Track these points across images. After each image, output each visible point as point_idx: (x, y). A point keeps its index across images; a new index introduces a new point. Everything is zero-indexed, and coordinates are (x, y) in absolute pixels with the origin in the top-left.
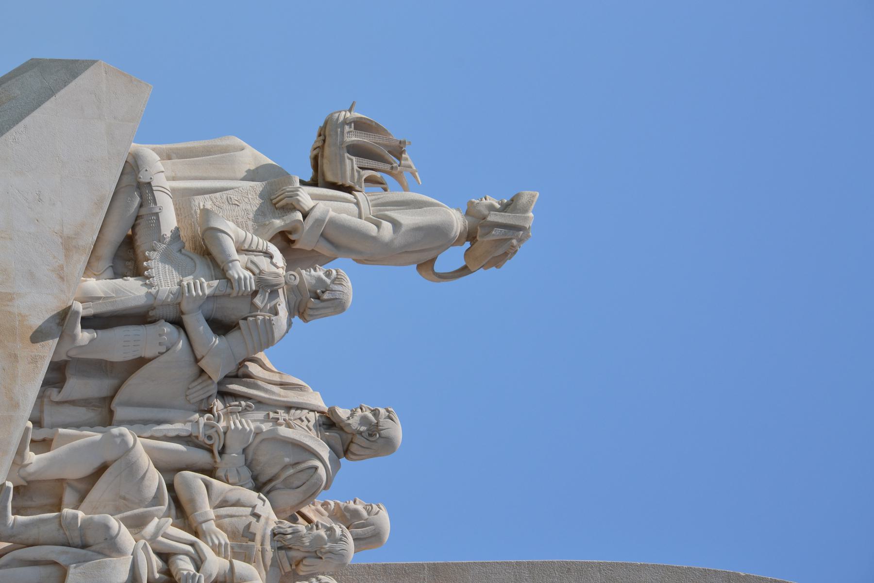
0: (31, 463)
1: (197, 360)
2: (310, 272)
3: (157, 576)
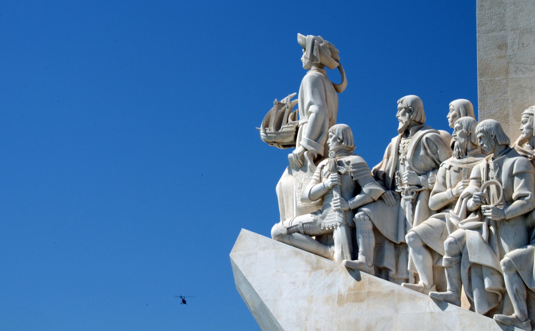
0: (423, 283)
1: (374, 201)
2: (330, 146)
3: (477, 216)
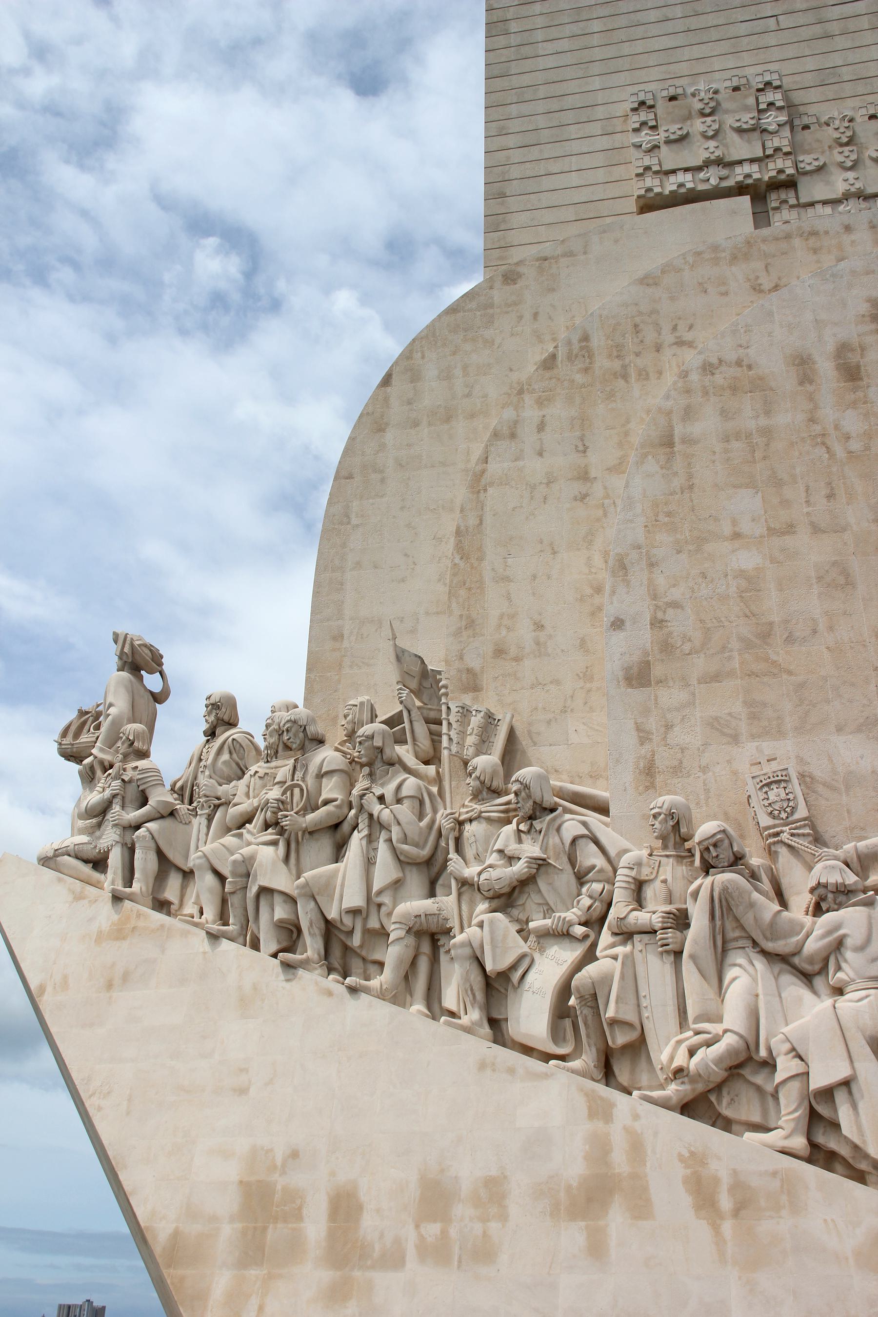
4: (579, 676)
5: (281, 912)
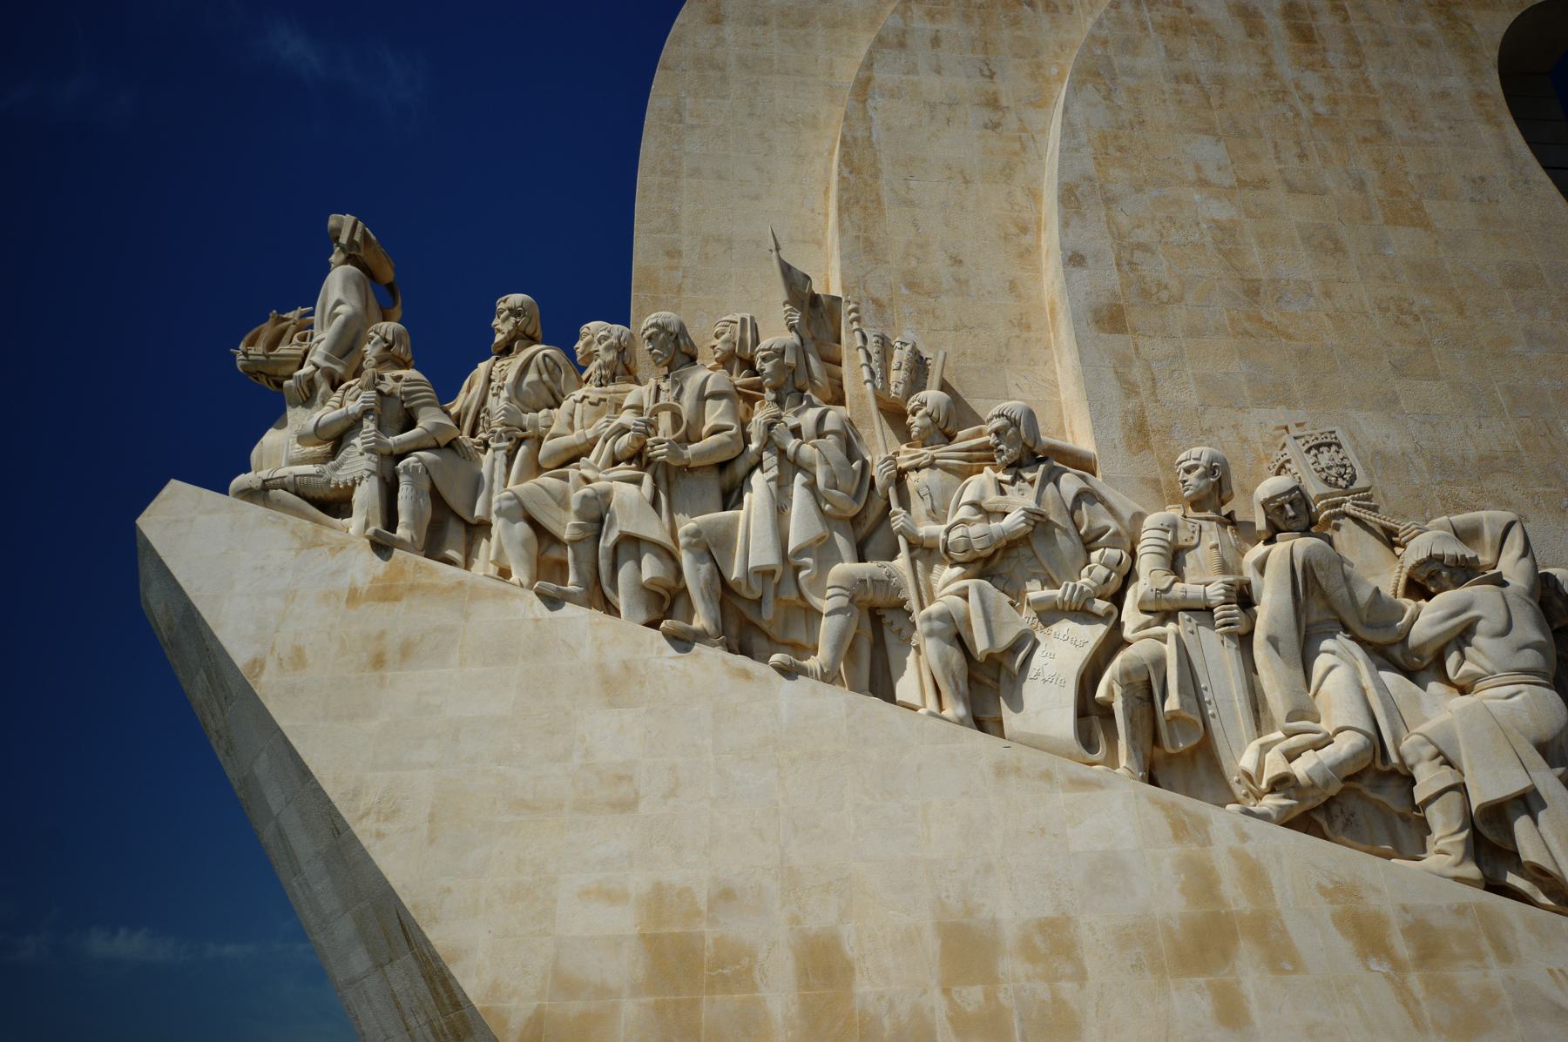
3: (633, 465)
4: (1013, 323)
5: (650, 567)
